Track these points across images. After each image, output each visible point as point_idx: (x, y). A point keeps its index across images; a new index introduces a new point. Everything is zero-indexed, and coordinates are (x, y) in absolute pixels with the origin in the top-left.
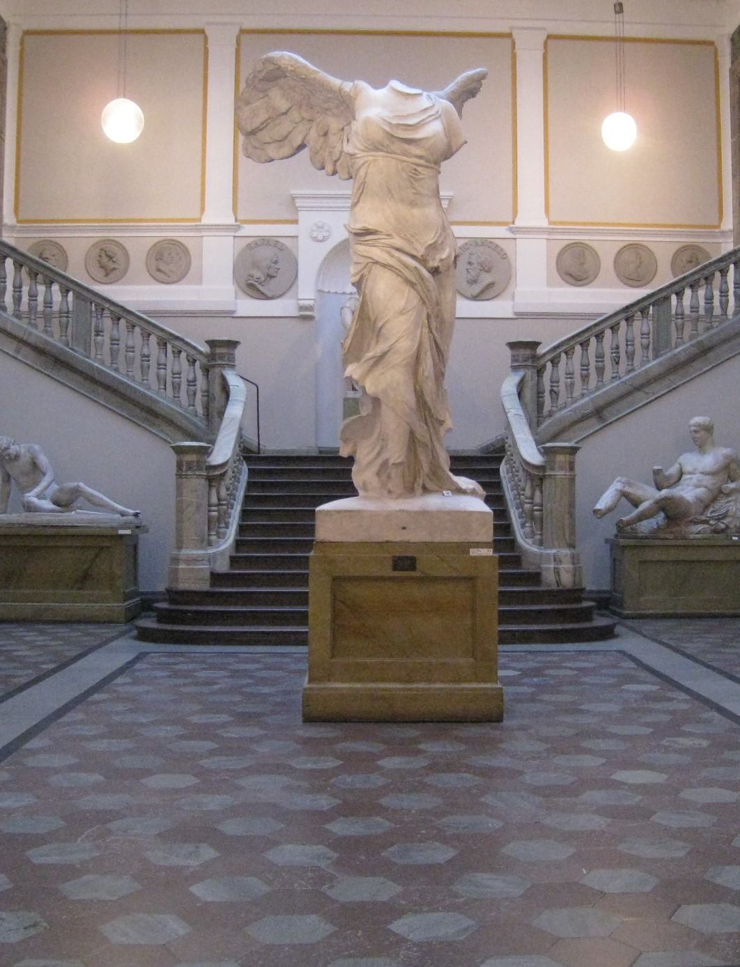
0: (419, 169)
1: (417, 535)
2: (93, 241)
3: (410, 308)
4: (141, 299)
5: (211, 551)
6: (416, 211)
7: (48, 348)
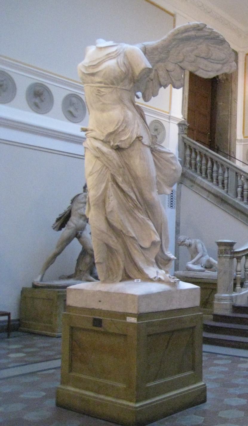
0: (102, 90)
1: (104, 307)
3: (94, 172)
6: (105, 115)
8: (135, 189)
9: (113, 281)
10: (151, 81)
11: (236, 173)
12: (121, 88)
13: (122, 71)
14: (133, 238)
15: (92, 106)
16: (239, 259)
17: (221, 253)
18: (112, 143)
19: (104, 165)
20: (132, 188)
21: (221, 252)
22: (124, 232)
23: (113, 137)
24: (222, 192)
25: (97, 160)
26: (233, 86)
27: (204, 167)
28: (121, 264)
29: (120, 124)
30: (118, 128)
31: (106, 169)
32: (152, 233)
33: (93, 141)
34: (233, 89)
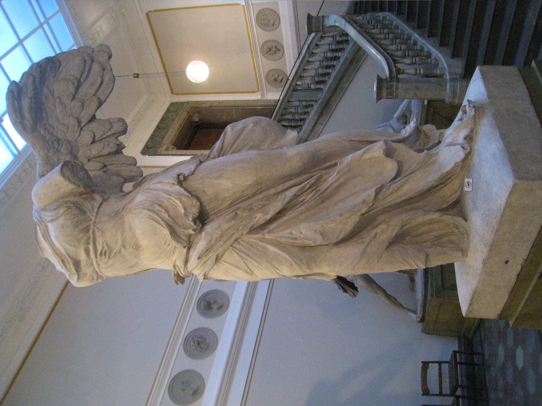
0: (99, 248)
5: (448, 77)
6: (144, 242)
7: (319, 111)
8: (281, 187)
9: (465, 235)
10: (108, 167)
11: (294, 91)
12: (95, 214)
13: (64, 213)
14: (377, 193)
15: (134, 266)
16: (399, 71)
17: (391, 94)
18: (191, 232)
19: (231, 246)
21: (390, 95)
22: (364, 210)
23: (180, 231)
24: (316, 106)
25: (223, 258)
26: (204, 105)
28: (428, 217)
29: (156, 217)
30: (163, 220)
31: (239, 243)
32: (367, 156)
33: (190, 266)
34: (208, 105)
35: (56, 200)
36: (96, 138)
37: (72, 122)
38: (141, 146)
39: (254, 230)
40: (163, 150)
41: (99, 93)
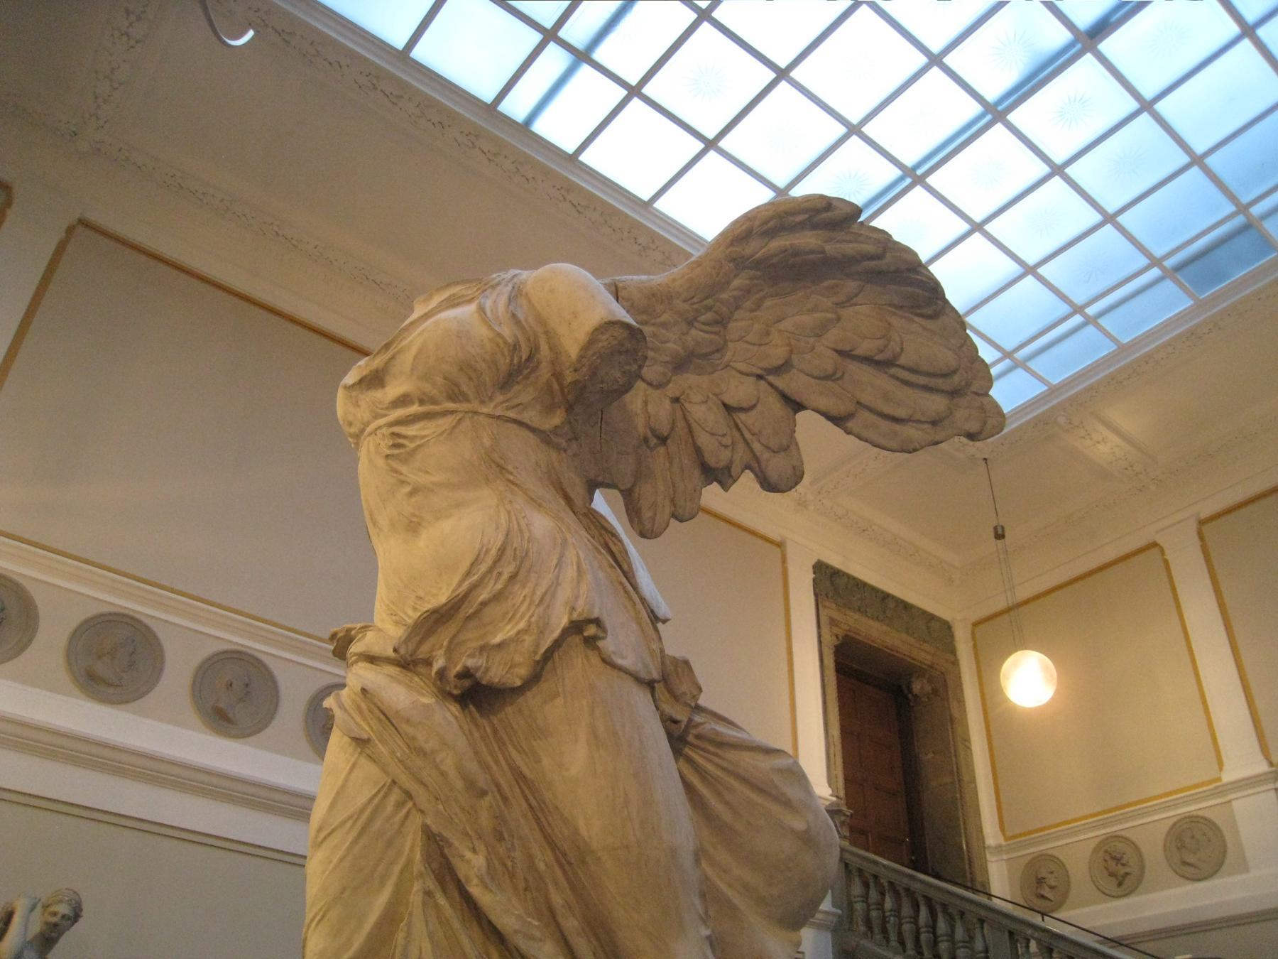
0: (410, 431)
2: (1093, 844)
4: (1148, 913)
6: (425, 542)
10: (662, 450)
11: (1011, 933)
12: (498, 413)
13: (499, 335)
18: (439, 663)
19: (394, 782)
20: (551, 917)
23: (444, 636)
25: (363, 760)
26: (954, 704)
27: (907, 927)
29: (483, 568)
30: (473, 587)
31: (400, 805)
34: (956, 713)
35: (542, 321)
36: (742, 416)
37: (777, 354)
38: (835, 561)
39: (436, 846)
40: (830, 611)
41: (867, 414)
